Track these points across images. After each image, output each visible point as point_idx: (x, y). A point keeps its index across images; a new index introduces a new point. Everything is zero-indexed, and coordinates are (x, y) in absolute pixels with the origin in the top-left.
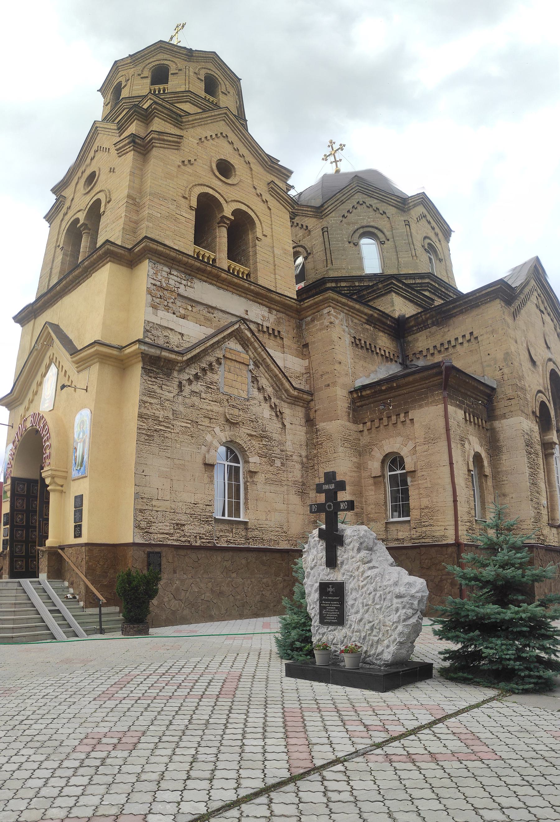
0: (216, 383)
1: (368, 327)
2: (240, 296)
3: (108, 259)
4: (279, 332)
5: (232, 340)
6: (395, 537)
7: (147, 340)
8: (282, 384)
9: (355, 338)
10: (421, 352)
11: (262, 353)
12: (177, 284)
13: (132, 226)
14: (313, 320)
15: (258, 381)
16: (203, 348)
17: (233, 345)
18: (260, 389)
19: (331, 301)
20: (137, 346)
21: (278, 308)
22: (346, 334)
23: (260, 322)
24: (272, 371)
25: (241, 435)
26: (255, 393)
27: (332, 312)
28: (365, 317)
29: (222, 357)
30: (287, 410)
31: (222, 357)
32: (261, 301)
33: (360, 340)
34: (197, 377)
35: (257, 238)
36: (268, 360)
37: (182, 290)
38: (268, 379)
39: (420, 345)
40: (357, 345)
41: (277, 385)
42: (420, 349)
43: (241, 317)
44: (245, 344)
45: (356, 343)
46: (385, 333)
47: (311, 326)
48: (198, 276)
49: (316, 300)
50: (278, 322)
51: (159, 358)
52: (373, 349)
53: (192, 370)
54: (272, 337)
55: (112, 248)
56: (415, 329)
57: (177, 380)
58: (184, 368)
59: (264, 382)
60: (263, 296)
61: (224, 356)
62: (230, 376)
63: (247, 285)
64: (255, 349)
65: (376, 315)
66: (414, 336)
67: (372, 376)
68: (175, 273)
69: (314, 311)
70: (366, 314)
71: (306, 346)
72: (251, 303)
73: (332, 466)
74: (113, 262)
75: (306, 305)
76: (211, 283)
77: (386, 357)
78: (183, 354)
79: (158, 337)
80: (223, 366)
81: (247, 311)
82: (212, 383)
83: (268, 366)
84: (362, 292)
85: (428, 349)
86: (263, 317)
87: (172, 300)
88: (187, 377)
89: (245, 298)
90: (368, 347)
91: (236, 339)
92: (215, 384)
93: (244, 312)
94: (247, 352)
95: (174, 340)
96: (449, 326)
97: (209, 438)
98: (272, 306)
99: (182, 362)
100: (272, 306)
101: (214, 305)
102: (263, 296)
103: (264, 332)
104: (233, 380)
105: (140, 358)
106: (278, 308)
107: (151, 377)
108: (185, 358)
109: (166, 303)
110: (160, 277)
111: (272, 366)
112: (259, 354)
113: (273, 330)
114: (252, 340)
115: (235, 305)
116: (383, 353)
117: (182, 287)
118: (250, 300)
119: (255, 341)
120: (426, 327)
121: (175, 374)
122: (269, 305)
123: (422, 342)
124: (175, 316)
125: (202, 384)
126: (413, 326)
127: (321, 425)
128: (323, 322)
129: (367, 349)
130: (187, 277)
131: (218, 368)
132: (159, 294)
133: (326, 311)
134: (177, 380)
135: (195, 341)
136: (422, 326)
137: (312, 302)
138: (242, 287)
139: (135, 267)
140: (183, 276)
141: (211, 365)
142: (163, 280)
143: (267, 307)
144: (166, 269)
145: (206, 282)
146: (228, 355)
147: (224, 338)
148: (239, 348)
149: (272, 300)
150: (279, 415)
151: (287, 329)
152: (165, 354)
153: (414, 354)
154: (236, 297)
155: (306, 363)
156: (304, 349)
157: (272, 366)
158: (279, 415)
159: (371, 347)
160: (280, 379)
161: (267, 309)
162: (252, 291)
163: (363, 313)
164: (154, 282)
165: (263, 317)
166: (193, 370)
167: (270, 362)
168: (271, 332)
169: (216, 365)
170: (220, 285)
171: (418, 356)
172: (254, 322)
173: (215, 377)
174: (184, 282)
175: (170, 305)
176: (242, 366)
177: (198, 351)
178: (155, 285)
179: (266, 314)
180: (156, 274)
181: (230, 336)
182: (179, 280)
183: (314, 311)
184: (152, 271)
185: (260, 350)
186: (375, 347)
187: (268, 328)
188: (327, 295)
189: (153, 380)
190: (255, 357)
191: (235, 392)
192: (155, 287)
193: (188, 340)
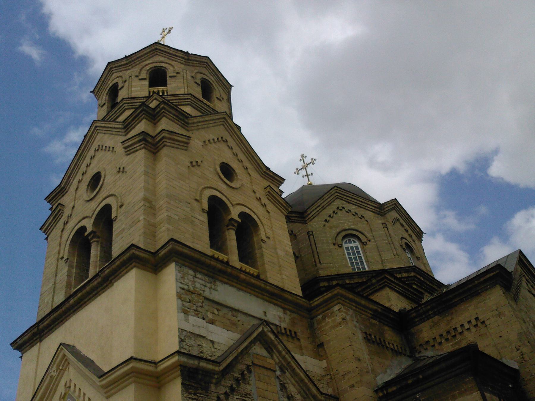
0: (250, 394)
1: (374, 321)
2: (257, 297)
3: (134, 264)
4: (295, 333)
5: (257, 344)
7: (182, 351)
8: (309, 390)
9: (365, 333)
10: (428, 342)
11: (287, 356)
12: (203, 287)
13: (151, 230)
14: (324, 318)
15: (286, 388)
16: (235, 355)
17: (258, 350)
19: (339, 297)
20: (176, 358)
21: (291, 308)
22: (358, 330)
23: (278, 323)
24: (296, 375)
27: (342, 309)
28: (371, 312)
29: (251, 364)
31: (251, 364)
32: (276, 302)
33: (370, 335)
35: (262, 240)
36: (293, 363)
37: (207, 293)
38: (294, 386)
40: (369, 340)
41: (304, 391)
42: (426, 340)
43: (261, 320)
44: (269, 347)
45: (368, 339)
46: (389, 327)
47: (323, 324)
48: (220, 278)
49: (326, 297)
50: (293, 322)
51: (196, 370)
52: (383, 343)
53: (227, 381)
54: (290, 339)
55: (137, 253)
56: (416, 320)
57: (215, 395)
58: (220, 381)
61: (252, 363)
62: (261, 385)
63: (263, 285)
64: (279, 352)
65: (380, 310)
66: (417, 328)
67: (388, 371)
68: (199, 276)
69: (325, 309)
70: (371, 310)
71: (321, 345)
72: (267, 303)
74: (138, 267)
75: (316, 303)
76: (231, 285)
77: (396, 351)
78: (219, 363)
79: (193, 346)
80: (253, 375)
81: (265, 313)
82: (246, 395)
83: (293, 370)
84: (360, 286)
85: (434, 339)
86: (280, 318)
87: (200, 304)
88: (223, 390)
89: (263, 299)
90: (379, 341)
91: (261, 343)
92: (249, 396)
93: (263, 314)
94: (272, 356)
95: (207, 349)
98: (286, 306)
99: (217, 373)
100: (286, 306)
101: (237, 308)
103: (282, 334)
105: (179, 372)
106: (291, 308)
107: (190, 393)
108: (221, 368)
109: (195, 307)
110: (187, 281)
111: (297, 370)
112: (284, 357)
113: (290, 331)
114: (276, 342)
115: (253, 306)
116: (391, 345)
117: (207, 290)
118: (267, 301)
119: (279, 343)
120: (428, 318)
121: (213, 387)
122: (283, 305)
123: (426, 331)
124: (204, 321)
125: (238, 397)
126: (415, 318)
128: (335, 320)
129: (378, 344)
130: (211, 279)
131: (250, 377)
132: (187, 298)
133: (336, 308)
134: (215, 395)
136: (424, 316)
137: (321, 300)
138: (259, 288)
139: (159, 271)
140: (207, 279)
141: (242, 374)
142: (190, 283)
143: (281, 307)
144: (191, 272)
145: (226, 283)
146: (256, 362)
147: (251, 343)
148: (264, 352)
149: (286, 300)
151: (300, 330)
152: (203, 364)
153: (421, 345)
154: (253, 298)
155: (324, 363)
156: (319, 349)
157: (297, 370)
159: (381, 341)
160: (306, 385)
161: (282, 310)
162: (268, 291)
163: (367, 308)
164: (182, 286)
165: (280, 318)
166: (228, 382)
167: (295, 366)
168: (288, 333)
169: (248, 374)
170: (239, 286)
171: (425, 346)
172: (273, 324)
173: (249, 387)
174: (208, 285)
175: (199, 309)
176: (270, 373)
177: (231, 358)
178: (183, 289)
179: (282, 315)
180: (183, 277)
181: (255, 339)
182: (203, 282)
183: (325, 309)
184: (179, 275)
185: (284, 353)
186: (384, 341)
187: (285, 329)
188: (336, 292)
189: (194, 397)
190: (280, 361)
192: (183, 291)
193: (219, 348)
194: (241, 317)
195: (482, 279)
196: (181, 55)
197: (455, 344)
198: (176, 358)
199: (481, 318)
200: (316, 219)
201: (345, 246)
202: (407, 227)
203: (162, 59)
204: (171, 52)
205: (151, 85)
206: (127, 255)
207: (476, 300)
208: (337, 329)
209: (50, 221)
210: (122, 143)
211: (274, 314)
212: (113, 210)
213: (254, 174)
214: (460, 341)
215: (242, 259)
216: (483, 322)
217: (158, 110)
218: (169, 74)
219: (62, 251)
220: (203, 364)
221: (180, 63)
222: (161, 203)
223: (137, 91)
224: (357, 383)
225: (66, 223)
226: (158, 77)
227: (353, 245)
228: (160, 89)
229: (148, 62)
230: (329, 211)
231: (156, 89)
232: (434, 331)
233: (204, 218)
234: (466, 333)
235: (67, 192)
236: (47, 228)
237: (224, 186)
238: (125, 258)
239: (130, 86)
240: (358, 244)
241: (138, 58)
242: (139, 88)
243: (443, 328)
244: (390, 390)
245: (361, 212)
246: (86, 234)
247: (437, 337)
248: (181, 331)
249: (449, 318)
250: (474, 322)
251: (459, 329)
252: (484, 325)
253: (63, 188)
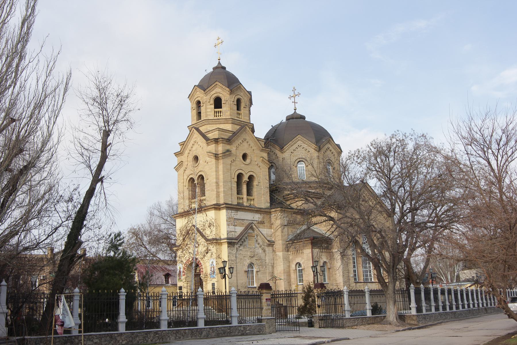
18: (259, 244)
25: (254, 260)
26: (257, 245)
30: (267, 249)
34: (241, 245)
37: (235, 217)
50: (263, 218)
59: (260, 241)
60: (259, 211)
97: (245, 262)
102: (259, 211)
104: (251, 243)
111: (262, 236)
127: (277, 253)
135: (239, 233)
148: (252, 231)
150: (264, 251)
152: (233, 241)
158: (264, 251)
191: (251, 246)
194: (245, 221)
198: (226, 241)
200: (287, 151)
201: (298, 166)
202: (333, 150)
203: (220, 90)
205: (215, 108)
211: (257, 217)
213: (258, 152)
215: (247, 195)
218: (222, 103)
219: (185, 183)
220: (233, 241)
222: (221, 184)
223: (209, 112)
225: (185, 171)
226: (218, 103)
227: (302, 165)
228: (219, 110)
230: (294, 147)
231: (217, 110)
233: (235, 185)
236: (177, 168)
237: (244, 165)
239: (206, 109)
240: (304, 165)
242: (210, 110)
245: (309, 149)
248: (227, 231)
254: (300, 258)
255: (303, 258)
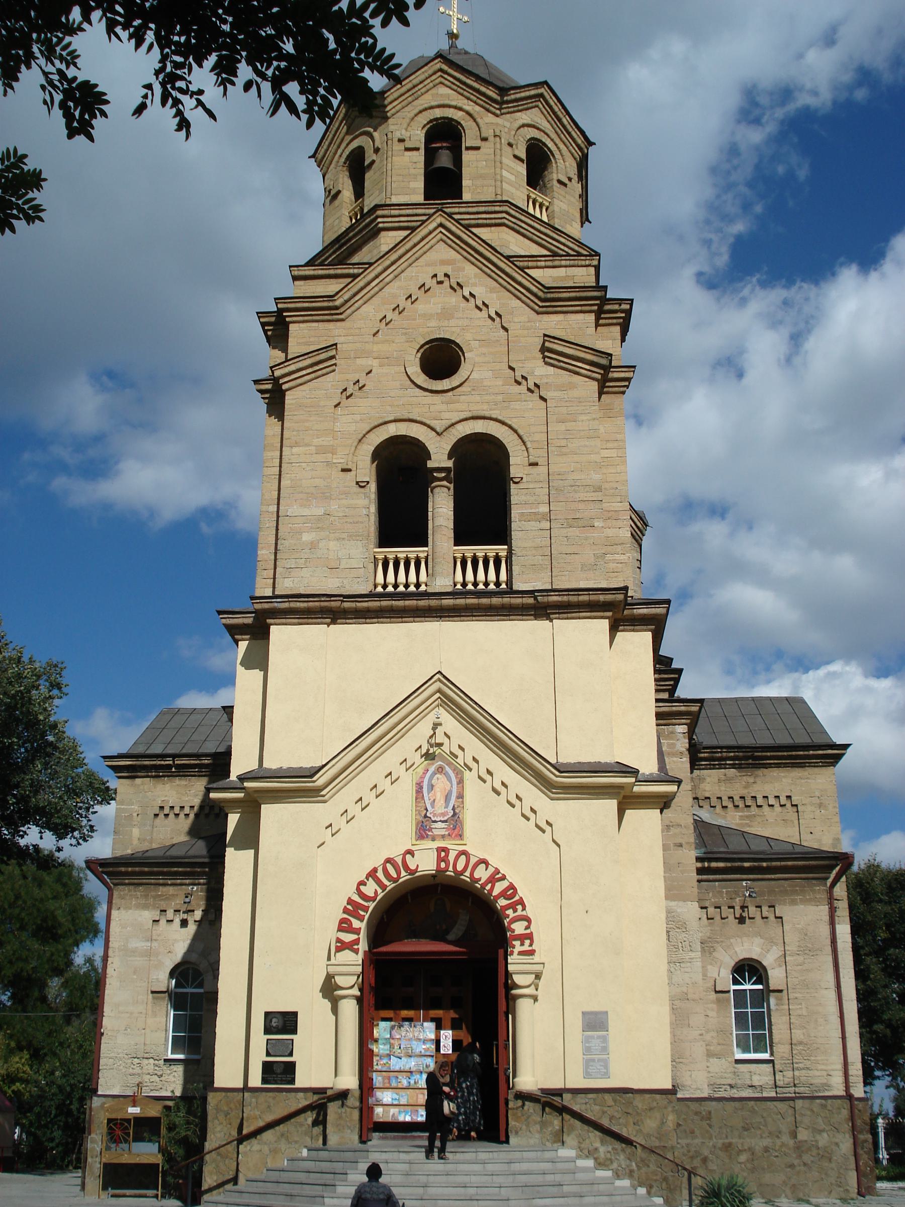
6: (749, 1083)
39: (707, 788)
73: (686, 970)
96: (756, 776)
128: (674, 745)
195: (821, 752)
196: (579, 142)
197: (747, 817)
199: (795, 800)
203: (545, 125)
204: (564, 121)
206: (609, 597)
207: (797, 773)
208: (675, 759)
209: (300, 365)
210: (545, 335)
212: (512, 461)
214: (754, 816)
216: (796, 806)
217: (616, 307)
221: (572, 155)
223: (510, 183)
224: (688, 843)
229: (524, 117)
231: (534, 194)
232: (723, 788)
234: (766, 808)
235: (343, 320)
238: (602, 598)
241: (516, 100)
242: (513, 178)
243: (737, 790)
244: (714, 864)
246: (430, 464)
247: (725, 798)
249: (751, 780)
250: (783, 800)
251: (760, 801)
252: (795, 809)
253: (337, 308)
254: (758, 941)
255: (772, 942)
